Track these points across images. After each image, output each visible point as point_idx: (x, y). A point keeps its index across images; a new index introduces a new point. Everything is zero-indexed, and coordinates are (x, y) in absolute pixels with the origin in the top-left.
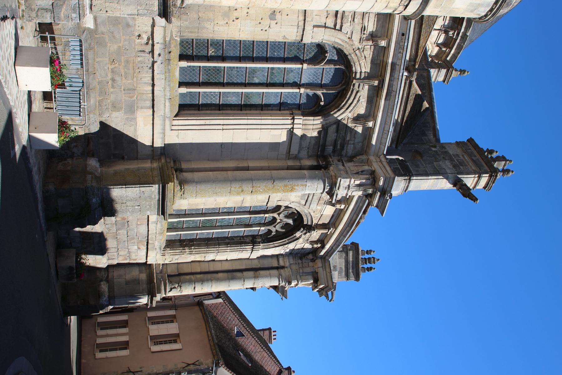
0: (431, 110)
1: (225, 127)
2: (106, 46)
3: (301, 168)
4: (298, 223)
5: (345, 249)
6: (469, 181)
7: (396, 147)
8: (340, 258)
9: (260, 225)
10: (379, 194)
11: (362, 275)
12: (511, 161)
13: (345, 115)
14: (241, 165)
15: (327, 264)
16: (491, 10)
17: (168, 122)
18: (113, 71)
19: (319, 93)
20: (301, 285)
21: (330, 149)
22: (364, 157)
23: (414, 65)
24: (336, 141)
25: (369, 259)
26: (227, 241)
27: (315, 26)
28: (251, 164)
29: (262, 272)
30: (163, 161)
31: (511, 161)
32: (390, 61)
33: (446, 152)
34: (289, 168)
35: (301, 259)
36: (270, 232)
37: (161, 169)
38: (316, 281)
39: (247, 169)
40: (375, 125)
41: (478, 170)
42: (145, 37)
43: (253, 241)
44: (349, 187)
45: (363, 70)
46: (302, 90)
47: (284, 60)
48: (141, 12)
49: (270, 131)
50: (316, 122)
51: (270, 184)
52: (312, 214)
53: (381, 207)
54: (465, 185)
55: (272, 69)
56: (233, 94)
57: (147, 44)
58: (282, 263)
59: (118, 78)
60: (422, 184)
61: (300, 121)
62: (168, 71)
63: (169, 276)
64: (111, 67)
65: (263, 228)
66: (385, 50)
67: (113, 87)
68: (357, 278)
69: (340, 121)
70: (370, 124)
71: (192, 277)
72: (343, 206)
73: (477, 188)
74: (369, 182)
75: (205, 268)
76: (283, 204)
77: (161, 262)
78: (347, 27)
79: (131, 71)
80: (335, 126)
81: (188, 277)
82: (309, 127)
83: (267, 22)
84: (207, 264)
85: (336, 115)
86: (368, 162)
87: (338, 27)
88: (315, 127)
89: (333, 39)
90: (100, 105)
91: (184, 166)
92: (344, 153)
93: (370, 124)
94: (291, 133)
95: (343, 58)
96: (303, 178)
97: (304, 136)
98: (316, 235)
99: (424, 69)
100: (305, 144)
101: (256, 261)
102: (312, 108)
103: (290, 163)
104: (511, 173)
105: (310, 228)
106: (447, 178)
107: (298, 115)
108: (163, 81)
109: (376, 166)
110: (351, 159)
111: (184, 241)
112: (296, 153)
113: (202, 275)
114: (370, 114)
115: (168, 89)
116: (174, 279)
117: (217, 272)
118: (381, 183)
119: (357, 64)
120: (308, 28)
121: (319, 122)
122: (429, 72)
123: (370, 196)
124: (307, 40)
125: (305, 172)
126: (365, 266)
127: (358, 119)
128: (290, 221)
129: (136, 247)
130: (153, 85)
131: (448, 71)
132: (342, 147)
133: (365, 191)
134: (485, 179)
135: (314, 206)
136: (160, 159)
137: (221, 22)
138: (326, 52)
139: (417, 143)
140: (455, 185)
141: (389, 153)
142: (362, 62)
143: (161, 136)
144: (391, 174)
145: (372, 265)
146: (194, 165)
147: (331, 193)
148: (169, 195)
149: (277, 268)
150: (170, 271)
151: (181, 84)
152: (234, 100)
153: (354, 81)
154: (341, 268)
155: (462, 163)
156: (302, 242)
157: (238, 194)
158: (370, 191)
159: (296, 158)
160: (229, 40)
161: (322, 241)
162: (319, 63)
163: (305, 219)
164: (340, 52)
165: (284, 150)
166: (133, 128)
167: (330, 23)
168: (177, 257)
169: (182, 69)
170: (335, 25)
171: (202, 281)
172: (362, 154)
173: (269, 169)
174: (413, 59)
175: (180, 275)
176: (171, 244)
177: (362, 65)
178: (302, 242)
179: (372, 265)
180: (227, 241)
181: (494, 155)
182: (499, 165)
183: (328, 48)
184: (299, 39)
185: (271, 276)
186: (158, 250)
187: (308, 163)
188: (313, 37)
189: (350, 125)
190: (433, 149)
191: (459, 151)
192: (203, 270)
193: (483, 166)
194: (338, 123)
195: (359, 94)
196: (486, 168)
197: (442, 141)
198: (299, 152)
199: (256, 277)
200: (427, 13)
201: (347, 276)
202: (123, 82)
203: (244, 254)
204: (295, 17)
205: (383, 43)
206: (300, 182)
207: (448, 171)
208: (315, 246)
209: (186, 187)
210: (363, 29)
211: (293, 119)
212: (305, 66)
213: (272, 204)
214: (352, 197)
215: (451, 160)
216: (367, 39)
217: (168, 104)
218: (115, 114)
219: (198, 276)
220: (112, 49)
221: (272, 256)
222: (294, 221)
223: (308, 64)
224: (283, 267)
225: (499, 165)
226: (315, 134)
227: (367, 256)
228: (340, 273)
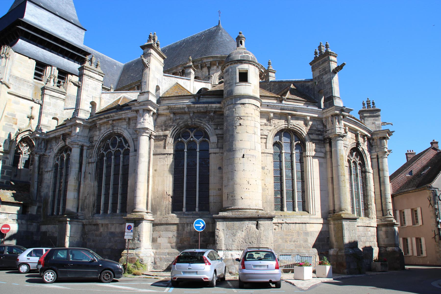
0: (295, 83)
1: (313, 189)
2: (280, 244)
3: (331, 152)
4: (355, 150)
5: (362, 118)
6: (334, 66)
7: (317, 103)
8: (368, 121)
9: (356, 169)
10: (343, 113)
11: (377, 107)
12: (321, 43)
13: (305, 131)
14: (331, 181)
15: (375, 133)
16: (257, 67)
17: (312, 217)
18: (290, 242)
19: (295, 144)
20: (386, 146)
21: (321, 137)
22: (324, 120)
23: (279, 98)
24: (317, 134)
25: (367, 104)
26: (364, 186)
27: (266, 148)
28: (330, 176)
29: (380, 167)
30: (330, 219)
31: (321, 43)
32: (280, 111)
33: (318, 77)
34: (331, 157)
35: (372, 146)
36: (360, 164)
37: (334, 220)
38: (384, 138)
39: (332, 178)
41: (327, 62)
42: (275, 227)
43: (364, 172)
44: (340, 128)
45: (284, 123)
46: (294, 152)
47: (281, 162)
48: (271, 229)
49: (314, 167)
50: (309, 145)
51: (340, 167)
52: (351, 143)
53: (349, 111)
54: (336, 68)
55: (285, 167)
56: (297, 186)
57: (278, 226)
58: (375, 156)
59: (293, 240)
60: (336, 92)
61: (309, 153)
62: (289, 216)
63: (383, 216)
64: (289, 242)
65: (358, 168)
66: (274, 113)
67: (297, 242)
68: (379, 110)
69: (307, 133)
70: (308, 118)
71: (383, 204)
72: (347, 128)
73: (336, 61)
74: (337, 118)
75: (378, 197)
76: (347, 158)
77: (376, 219)
78: (266, 133)
79: (290, 233)
80: (310, 135)
81: (384, 206)
82: (311, 147)
83: (265, 170)
84: (376, 196)
85: (305, 135)
86: (327, 118)
87: (266, 137)
88: (311, 145)
89: (271, 139)
90: (305, 248)
91: (332, 209)
92: (322, 130)
93: (308, 118)
94: (314, 157)
95: (279, 133)
96: (336, 151)
97: (315, 151)
98: (361, 140)
99: (270, 84)
100: (319, 150)
101: (374, 170)
102: (302, 147)
103: (328, 156)
104: (328, 44)
105: (358, 144)
106: (333, 78)
107: (305, 154)
108: (294, 219)
109: (329, 114)
110: (325, 126)
111: (365, 208)
112: (323, 154)
113: (383, 199)
114: (304, 118)
115: (297, 216)
116: (385, 213)
117: (381, 191)
118: (338, 112)
119: (281, 127)
120: (267, 151)
121: (308, 143)
122: (271, 81)
123: (344, 116)
124: (272, 151)
125: (333, 150)
126: (372, 106)
127: (306, 124)
128: (354, 153)
129: (369, 232)
130: (296, 223)
131: (270, 72)
132: (319, 131)
133: (341, 120)
134: (332, 58)
135: (347, 143)
136: (329, 221)
137: (267, 191)
138: (276, 141)
139: (314, 91)
140: (336, 73)
141: (320, 107)
142: (280, 124)
143: (318, 219)
144: (334, 107)
145: (371, 102)
146: (331, 204)
147: (343, 136)
148: (347, 216)
149: (378, 159)
150: (380, 214)
151: (294, 210)
152: (300, 185)
153: (289, 127)
154: (373, 120)
155: (324, 69)
156: (364, 146)
157: (345, 183)
158: (342, 117)
159: (325, 153)
160: (274, 187)
161: (364, 136)
162: (281, 145)
163: (353, 147)
164: (276, 135)
165: (322, 160)
166: (315, 233)
167: (264, 141)
168: (373, 212)
169: (288, 210)
170: (265, 138)
171: (386, 198)
172: (322, 121)
173: (332, 167)
174: (276, 98)
175: (382, 210)
176: (367, 215)
177: (281, 124)
178: (364, 146)
179: (371, 102)
180: (364, 186)
181: (318, 52)
182: (323, 50)
183: (275, 141)
184: (272, 155)
185: (382, 162)
186: (370, 221)
187: (328, 148)
188: (271, 149)
189: (309, 128)
190: (317, 83)
191: (317, 71)
192: (380, 198)
193: (325, 59)
194: (308, 134)
195: (295, 125)
196: (326, 57)
197: (311, 77)
198: (323, 152)
199: (383, 170)
200: (259, 97)
201: (378, 116)
202: (295, 237)
203: (370, 176)
205: (272, 115)
206: (339, 152)
207: (329, 77)
208: (366, 139)
209: (343, 208)
210: (266, 125)
211: (307, 156)
212: (283, 151)
213: (347, 165)
214: (345, 125)
215: (323, 75)
216: (270, 122)
217: (304, 217)
218: (309, 241)
219: (383, 200)
220: (281, 242)
221: (371, 161)
222: (354, 152)
223: (282, 150)
224: (377, 156)
225: (324, 50)
226: (314, 145)
227: (366, 105)
228: (376, 120)
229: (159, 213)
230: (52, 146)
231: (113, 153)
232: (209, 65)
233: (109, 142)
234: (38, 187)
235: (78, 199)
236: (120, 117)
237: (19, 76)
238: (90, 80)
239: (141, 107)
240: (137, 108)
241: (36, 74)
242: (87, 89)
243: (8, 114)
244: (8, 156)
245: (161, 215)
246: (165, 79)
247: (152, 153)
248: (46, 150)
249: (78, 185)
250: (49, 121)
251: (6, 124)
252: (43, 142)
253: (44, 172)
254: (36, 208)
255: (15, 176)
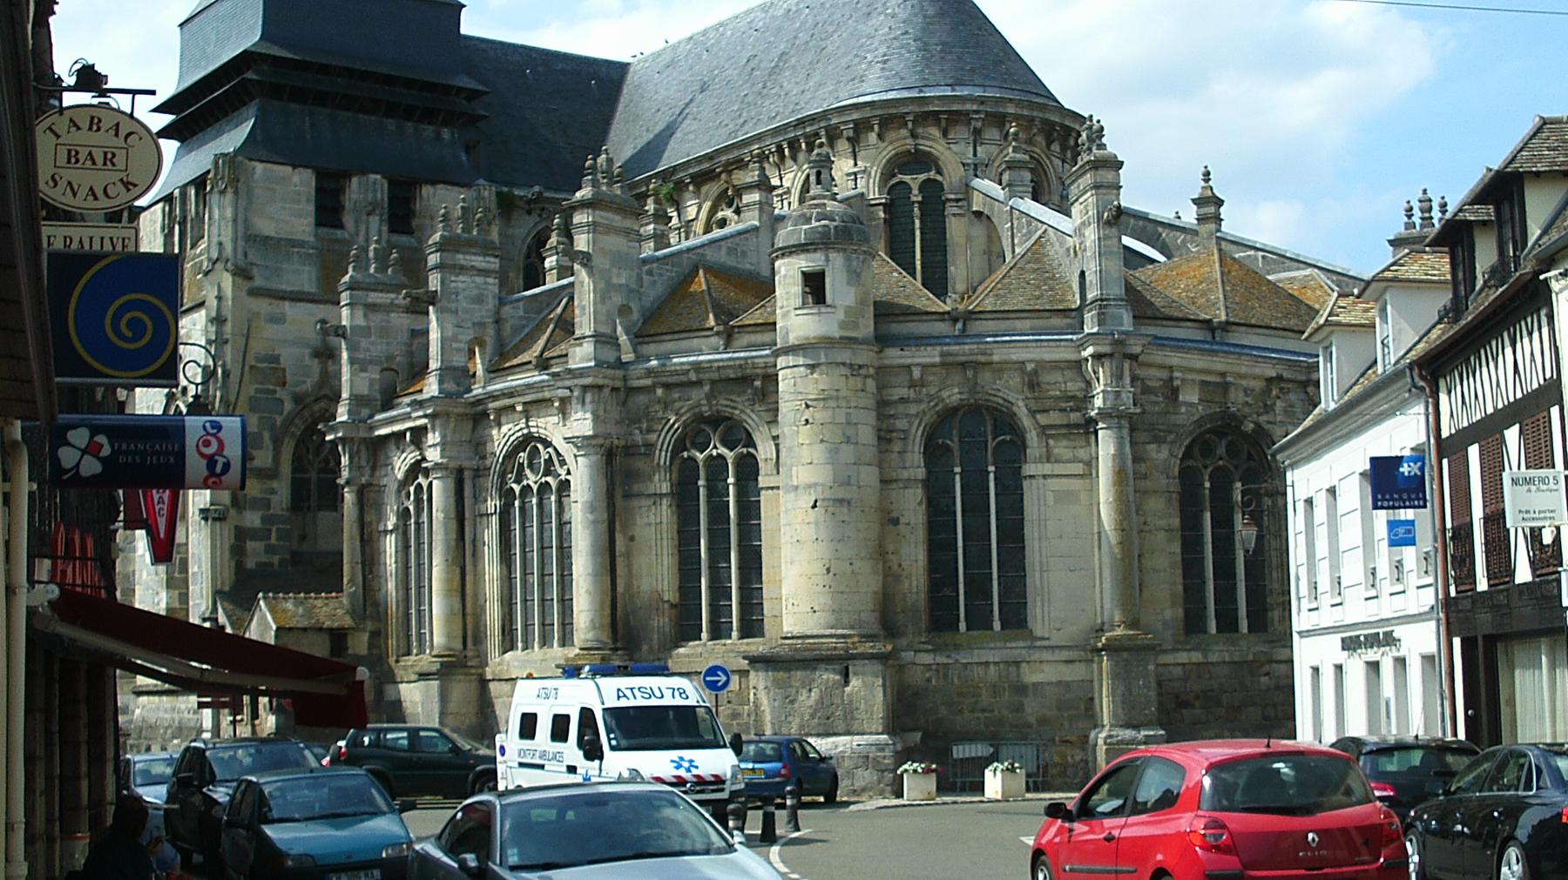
18: (972, 711)
21: (1075, 417)
24: (1063, 410)
25: (1422, 211)
40: (1031, 361)
64: (967, 714)
78: (901, 424)
92: (1080, 395)
124: (921, 473)
132: (1073, 398)
137: (907, 584)
202: (985, 699)
204: (894, 493)
218: (1028, 710)
229: (645, 648)
230: (388, 457)
231: (535, 488)
232: (851, 133)
233: (523, 456)
234: (364, 577)
235: (464, 615)
236: (540, 396)
237: (273, 234)
238: (461, 278)
239: (576, 381)
240: (568, 383)
241: (320, 209)
242: (453, 306)
243: (258, 359)
244: (275, 484)
245: (651, 650)
246: (650, 273)
247: (618, 494)
248: (374, 469)
249: (458, 577)
250: (372, 381)
251: (257, 391)
252: (363, 448)
253: (375, 535)
254: (365, 637)
255: (303, 538)
